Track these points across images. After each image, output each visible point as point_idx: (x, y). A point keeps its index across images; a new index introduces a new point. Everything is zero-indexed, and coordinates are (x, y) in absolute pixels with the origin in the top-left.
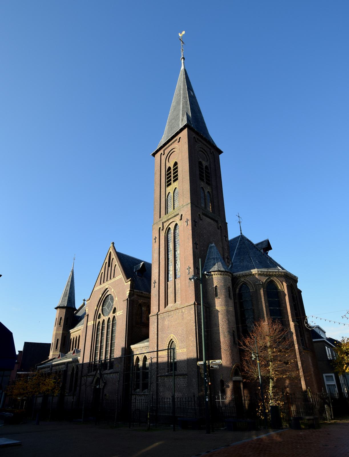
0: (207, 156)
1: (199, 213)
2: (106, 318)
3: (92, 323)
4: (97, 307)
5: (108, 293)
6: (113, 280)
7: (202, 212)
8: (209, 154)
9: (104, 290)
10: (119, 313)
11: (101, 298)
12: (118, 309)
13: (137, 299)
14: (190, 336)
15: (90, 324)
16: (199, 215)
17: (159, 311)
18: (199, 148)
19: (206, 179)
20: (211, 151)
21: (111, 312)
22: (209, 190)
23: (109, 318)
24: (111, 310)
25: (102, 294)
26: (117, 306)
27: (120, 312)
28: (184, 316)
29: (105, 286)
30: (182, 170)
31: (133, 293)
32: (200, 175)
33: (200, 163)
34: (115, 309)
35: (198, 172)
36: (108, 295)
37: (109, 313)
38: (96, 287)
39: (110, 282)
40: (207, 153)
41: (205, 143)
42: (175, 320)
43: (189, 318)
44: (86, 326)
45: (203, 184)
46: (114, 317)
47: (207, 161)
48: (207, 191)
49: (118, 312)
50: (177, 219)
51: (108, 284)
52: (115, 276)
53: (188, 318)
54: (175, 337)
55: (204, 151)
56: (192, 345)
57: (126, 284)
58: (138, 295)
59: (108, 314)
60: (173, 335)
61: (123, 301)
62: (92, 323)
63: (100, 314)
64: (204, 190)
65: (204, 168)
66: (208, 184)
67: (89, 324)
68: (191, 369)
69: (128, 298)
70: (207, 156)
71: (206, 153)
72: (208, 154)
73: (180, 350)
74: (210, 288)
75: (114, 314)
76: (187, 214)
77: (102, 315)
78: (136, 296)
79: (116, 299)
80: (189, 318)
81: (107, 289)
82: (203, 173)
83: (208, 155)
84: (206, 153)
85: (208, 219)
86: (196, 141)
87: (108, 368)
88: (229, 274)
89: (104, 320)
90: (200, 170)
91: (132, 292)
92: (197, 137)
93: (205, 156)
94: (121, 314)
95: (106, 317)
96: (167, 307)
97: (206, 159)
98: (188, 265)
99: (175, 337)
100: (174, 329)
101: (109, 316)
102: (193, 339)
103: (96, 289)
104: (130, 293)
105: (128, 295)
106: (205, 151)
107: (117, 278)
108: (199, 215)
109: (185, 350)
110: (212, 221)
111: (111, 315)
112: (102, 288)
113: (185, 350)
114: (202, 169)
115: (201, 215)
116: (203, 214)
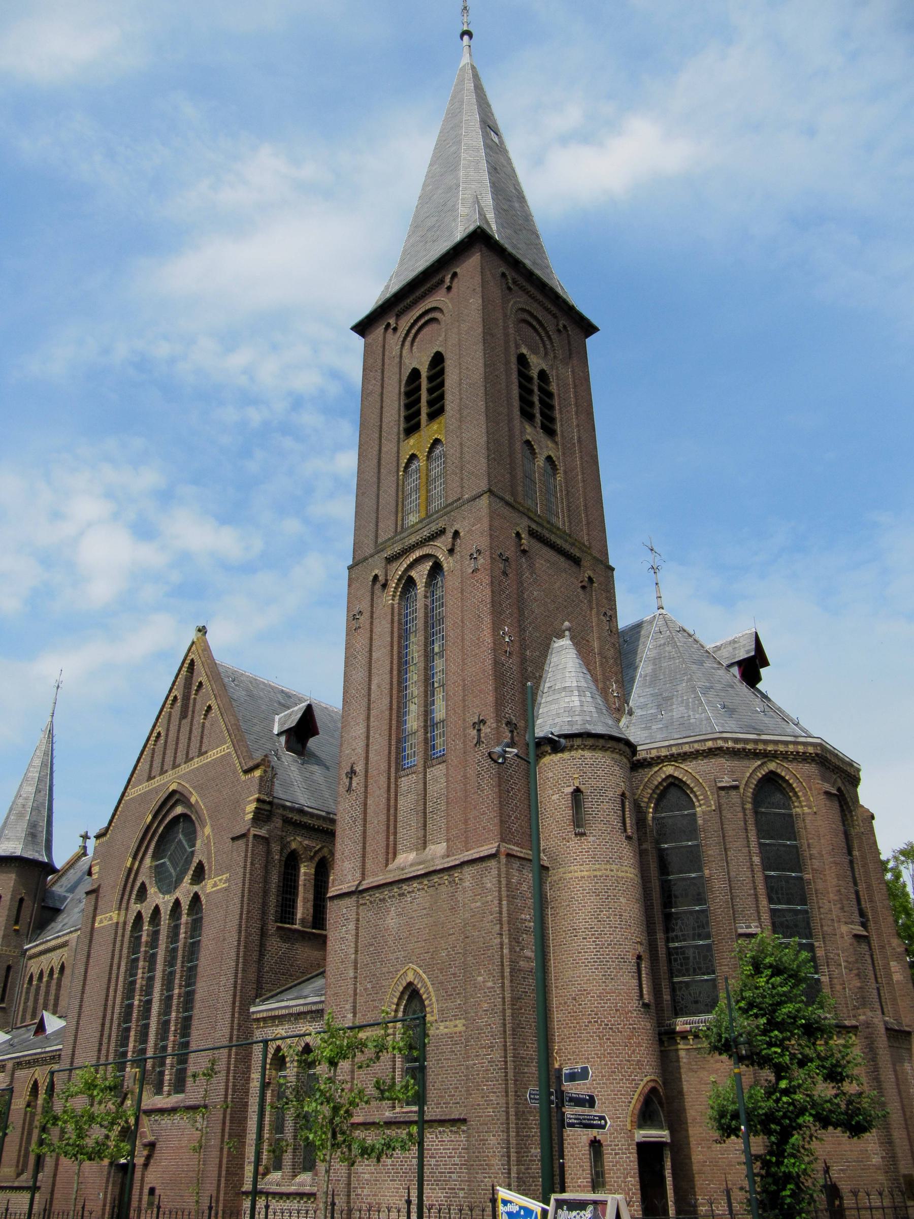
0: (545, 339)
1: (518, 529)
2: (165, 901)
3: (111, 919)
4: (134, 858)
5: (179, 810)
6: (196, 763)
7: (529, 527)
8: (551, 333)
9: (162, 795)
10: (215, 885)
11: (149, 827)
12: (210, 868)
13: (284, 834)
14: (480, 974)
15: (106, 923)
16: (518, 535)
17: (363, 876)
18: (520, 312)
19: (542, 414)
20: (558, 325)
21: (185, 880)
22: (551, 453)
23: (177, 903)
24: (184, 872)
25: (153, 813)
26: (209, 858)
27: (220, 880)
28: (460, 896)
29: (164, 784)
30: (461, 380)
31: (270, 811)
32: (522, 398)
33: (522, 360)
34: (200, 867)
35: (515, 391)
36: (177, 818)
37: (179, 881)
38: (133, 788)
39: (184, 769)
40: (544, 329)
41: (540, 297)
42: (425, 912)
43: (479, 904)
44: (89, 929)
45: (532, 432)
46: (196, 898)
47: (546, 354)
48: (545, 454)
49: (210, 878)
50: (439, 549)
51: (180, 777)
52: (204, 749)
53: (473, 905)
54: (424, 976)
55: (534, 323)
56: (485, 1006)
57: (243, 777)
58: (287, 821)
59: (176, 888)
60: (415, 967)
61: (233, 839)
62: (111, 919)
63: (143, 885)
64: (534, 449)
65: (535, 376)
66: (550, 432)
67: (101, 922)
68: (483, 1097)
69: (249, 830)
70: (545, 339)
71: (540, 330)
72: (547, 333)
73: (442, 1026)
74: (555, 797)
75: (196, 888)
76: (473, 528)
77: (152, 890)
78: (278, 823)
79: (208, 830)
80: (479, 904)
81: (174, 792)
82: (531, 392)
83: (549, 337)
84: (540, 330)
85: (549, 550)
86: (509, 289)
87: (166, 1089)
88: (622, 746)
89: (157, 910)
90: (520, 383)
91: (267, 807)
92: (511, 275)
93: (537, 338)
94: (222, 886)
95: (167, 897)
96: (390, 867)
97: (542, 349)
98: (477, 711)
99: (424, 976)
100: (419, 945)
101: (178, 894)
102: (490, 984)
103: (133, 793)
104: (257, 811)
105: (251, 816)
106: (539, 322)
107: (214, 754)
108: (518, 535)
109: (460, 1025)
110: (562, 559)
111: (185, 891)
112: (156, 790)
113: (460, 1025)
114: (530, 379)
115: (523, 536)
116: (532, 533)
